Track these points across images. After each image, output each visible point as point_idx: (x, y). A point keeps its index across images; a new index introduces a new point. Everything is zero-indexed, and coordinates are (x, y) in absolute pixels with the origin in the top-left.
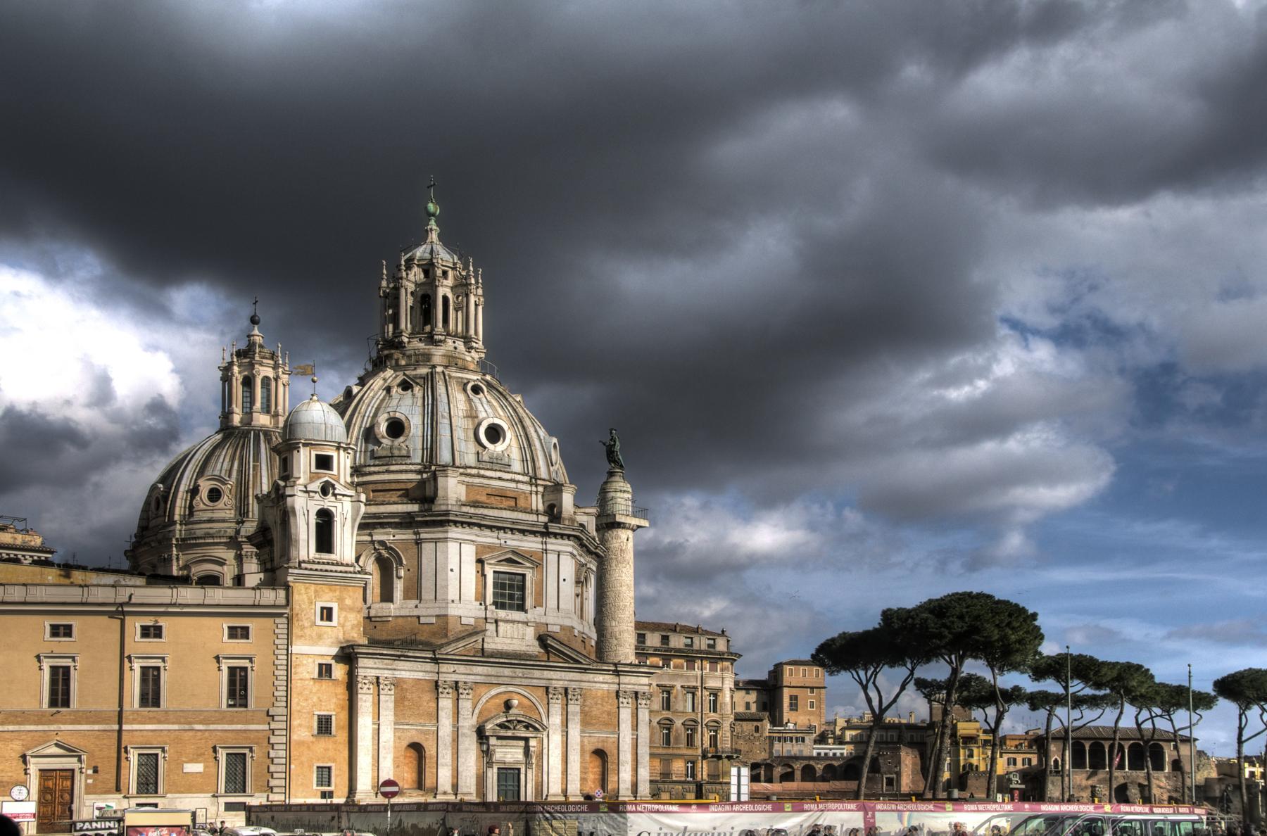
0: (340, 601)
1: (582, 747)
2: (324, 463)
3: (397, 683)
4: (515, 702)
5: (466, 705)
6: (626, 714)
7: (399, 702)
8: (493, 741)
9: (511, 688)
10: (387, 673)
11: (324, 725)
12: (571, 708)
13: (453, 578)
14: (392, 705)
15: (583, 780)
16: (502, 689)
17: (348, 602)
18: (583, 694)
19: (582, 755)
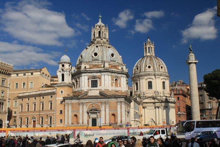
0: (64, 89)
1: (109, 114)
2: (63, 66)
3: (72, 104)
4: (94, 105)
5: (85, 107)
6: (119, 106)
7: (72, 107)
8: (90, 113)
9: (94, 103)
10: (70, 102)
11: (61, 112)
12: (106, 106)
13: (83, 83)
14: (71, 108)
15: (110, 120)
16: (91, 103)
17: (65, 90)
18: (109, 103)
19: (109, 115)
